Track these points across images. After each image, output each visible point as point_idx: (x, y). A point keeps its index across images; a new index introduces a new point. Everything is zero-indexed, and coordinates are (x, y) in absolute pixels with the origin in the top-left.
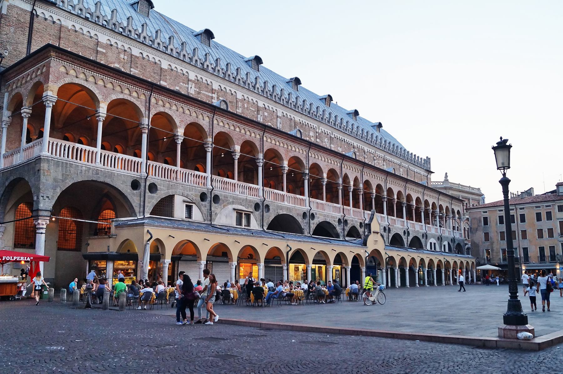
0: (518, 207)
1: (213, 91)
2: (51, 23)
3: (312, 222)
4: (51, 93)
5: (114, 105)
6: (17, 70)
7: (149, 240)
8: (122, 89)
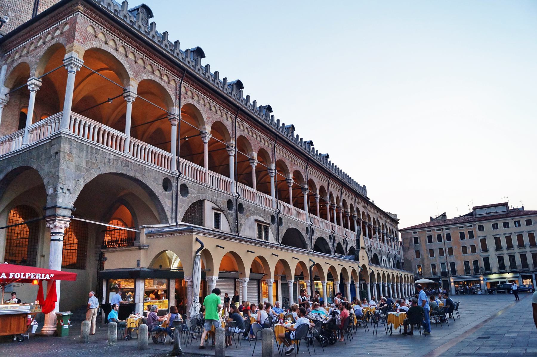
0: (444, 227)
3: (313, 237)
4: (76, 55)
7: (198, 251)
8: (153, 69)
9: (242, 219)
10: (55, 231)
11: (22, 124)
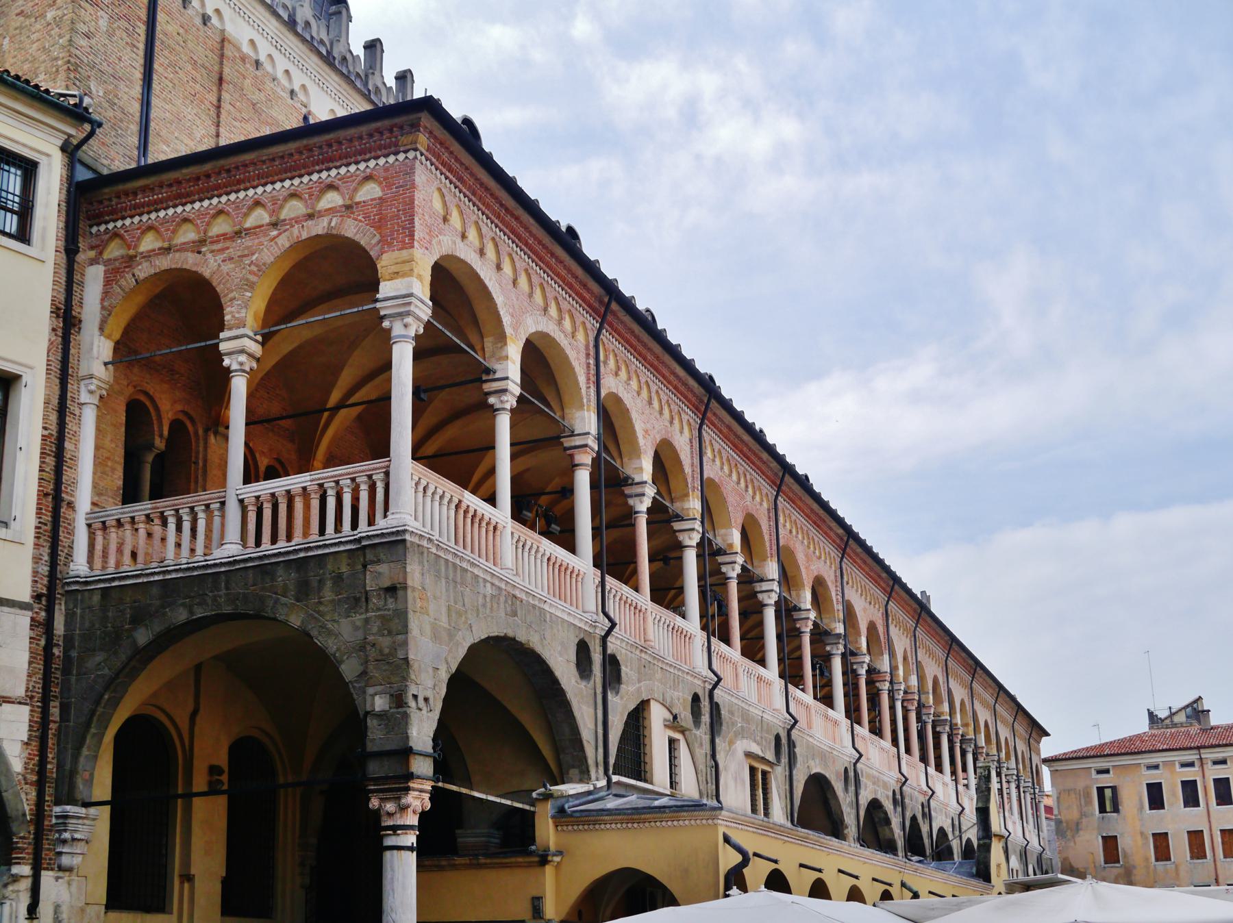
0: (1209, 755)
2: (198, 21)
6: (178, 182)
10: (400, 822)
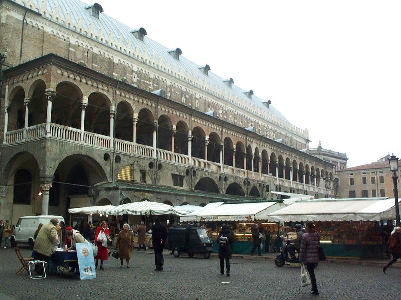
1: (149, 79)
2: (37, 30)
5: (94, 97)
9: (160, 173)
11: (22, 126)
